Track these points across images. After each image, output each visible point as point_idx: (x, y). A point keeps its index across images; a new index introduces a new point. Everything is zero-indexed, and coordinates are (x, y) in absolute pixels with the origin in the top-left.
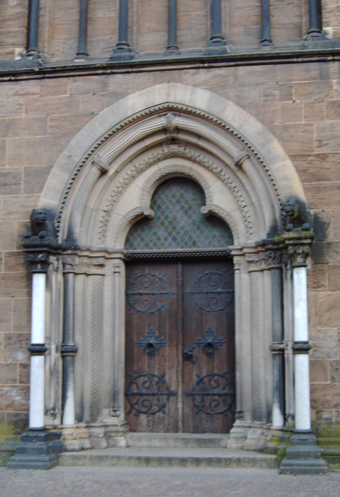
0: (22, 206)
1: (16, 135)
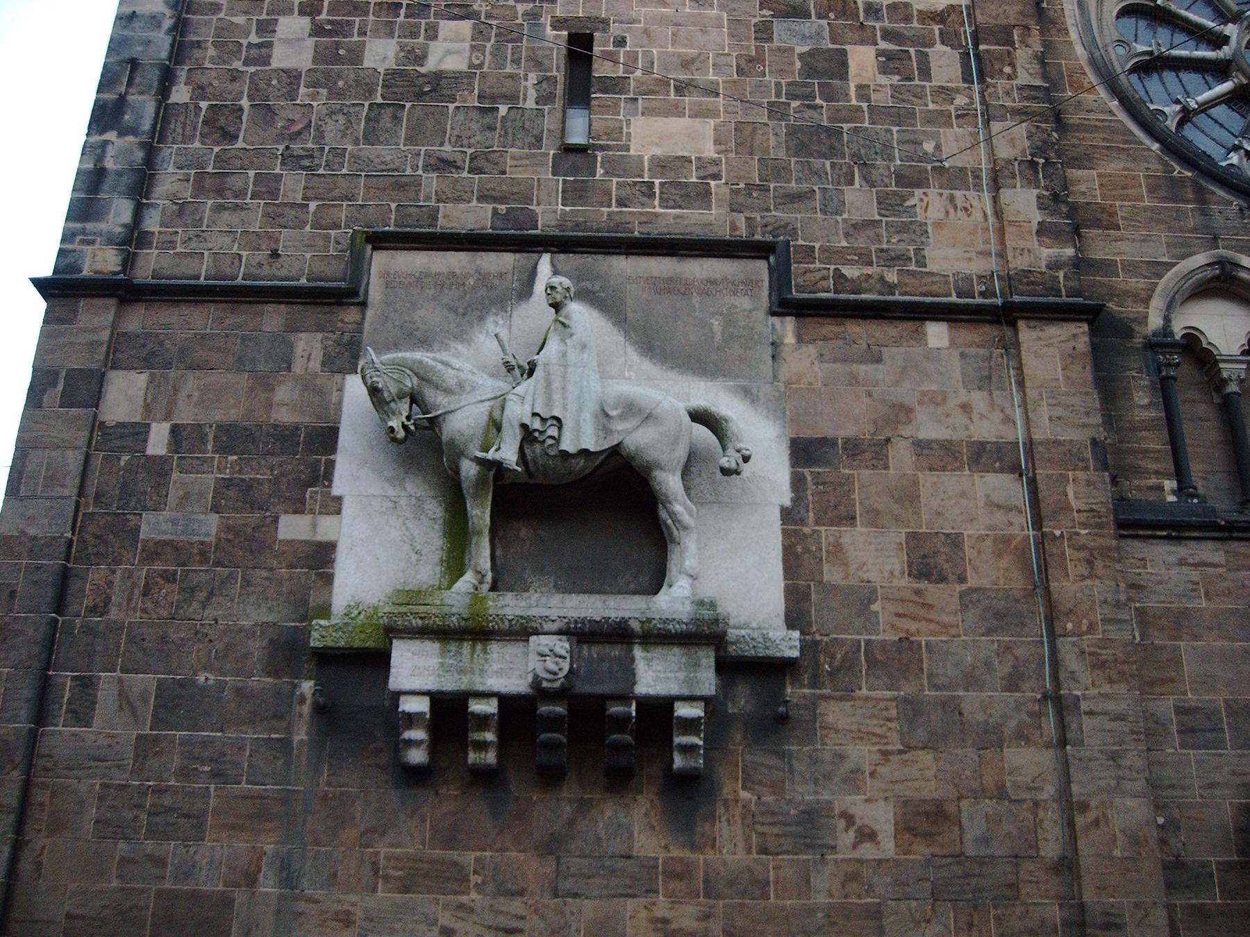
0: (1234, 773)
1: (1196, 637)
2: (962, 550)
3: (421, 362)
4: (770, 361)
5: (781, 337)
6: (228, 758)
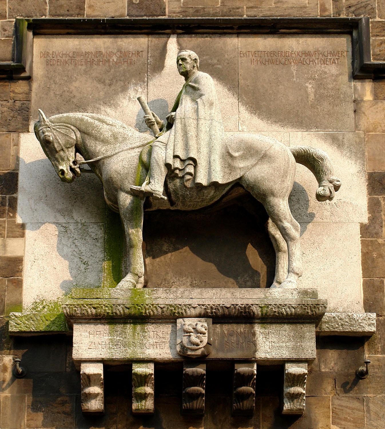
3: (82, 120)
4: (352, 115)
5: (362, 96)
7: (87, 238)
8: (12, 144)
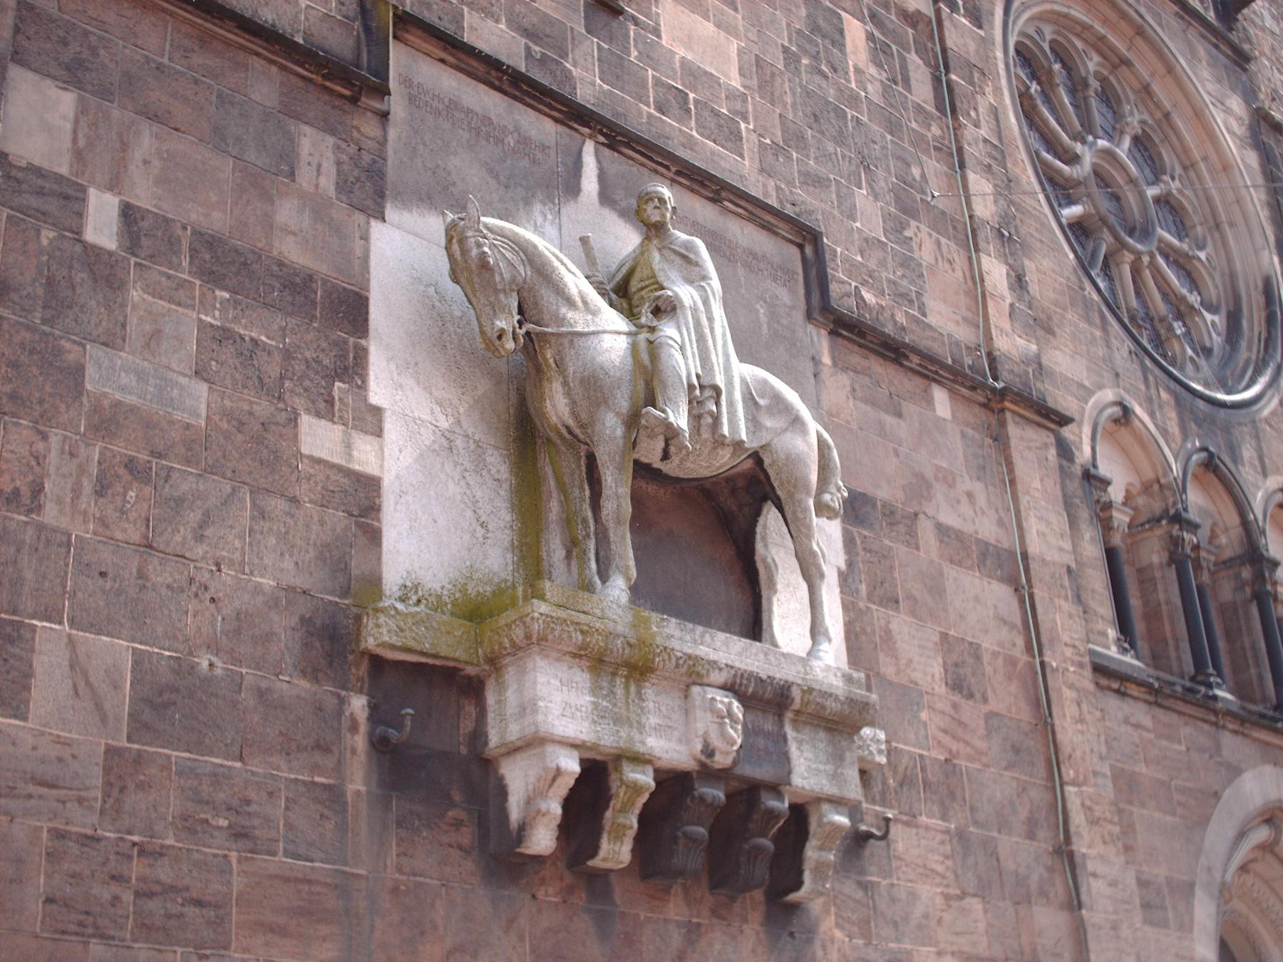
2: (982, 664)
3: (535, 247)
4: (812, 380)
6: (253, 808)
7: (484, 472)
8: (357, 235)
